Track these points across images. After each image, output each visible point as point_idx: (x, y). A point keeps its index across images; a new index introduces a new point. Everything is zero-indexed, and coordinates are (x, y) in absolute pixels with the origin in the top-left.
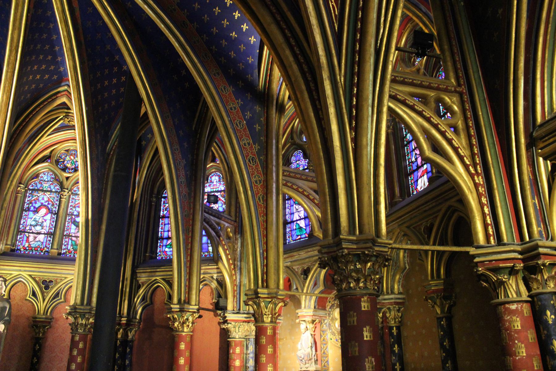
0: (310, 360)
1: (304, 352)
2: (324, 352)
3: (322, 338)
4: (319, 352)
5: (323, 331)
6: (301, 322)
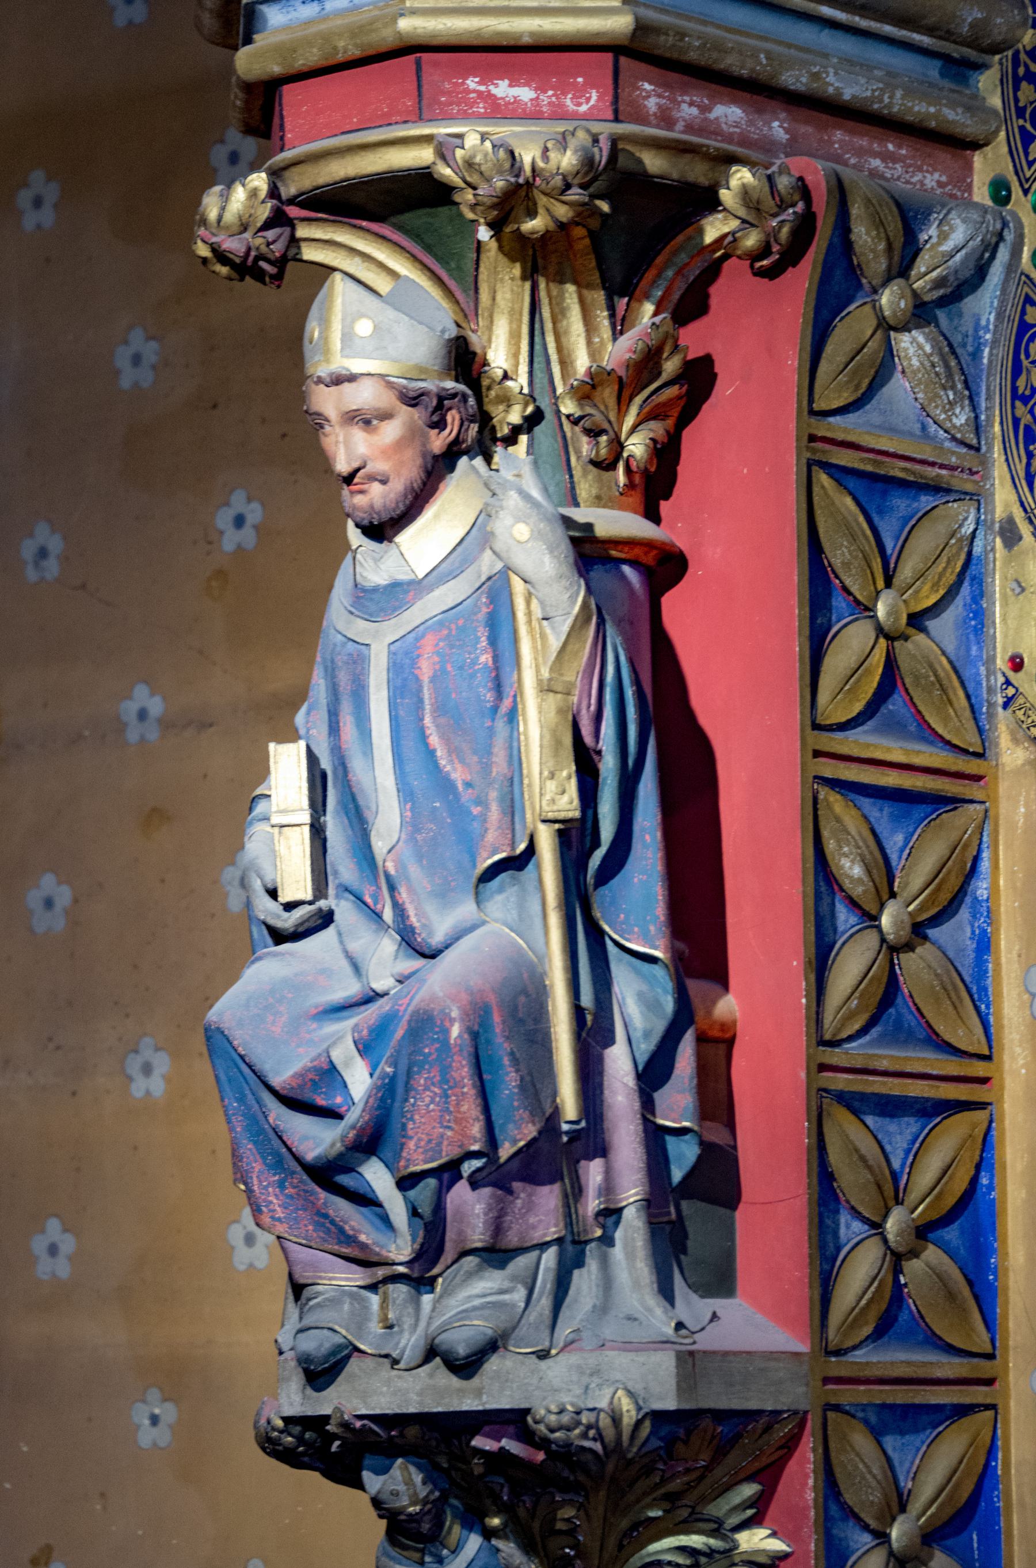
0: (559, 1154)
1: (384, 962)
2: (886, 995)
3: (852, 644)
4: (761, 995)
5: (877, 485)
6: (323, 242)
